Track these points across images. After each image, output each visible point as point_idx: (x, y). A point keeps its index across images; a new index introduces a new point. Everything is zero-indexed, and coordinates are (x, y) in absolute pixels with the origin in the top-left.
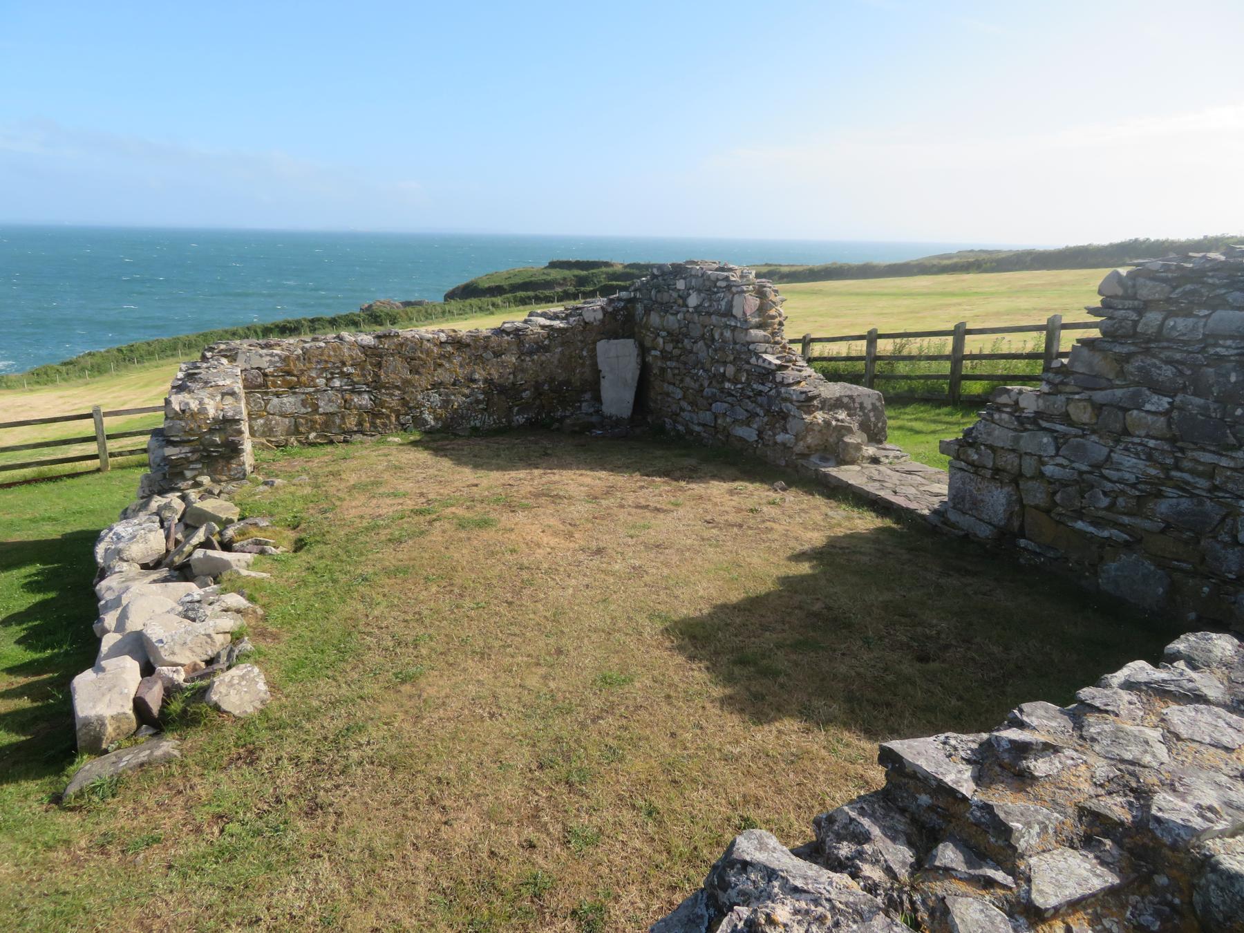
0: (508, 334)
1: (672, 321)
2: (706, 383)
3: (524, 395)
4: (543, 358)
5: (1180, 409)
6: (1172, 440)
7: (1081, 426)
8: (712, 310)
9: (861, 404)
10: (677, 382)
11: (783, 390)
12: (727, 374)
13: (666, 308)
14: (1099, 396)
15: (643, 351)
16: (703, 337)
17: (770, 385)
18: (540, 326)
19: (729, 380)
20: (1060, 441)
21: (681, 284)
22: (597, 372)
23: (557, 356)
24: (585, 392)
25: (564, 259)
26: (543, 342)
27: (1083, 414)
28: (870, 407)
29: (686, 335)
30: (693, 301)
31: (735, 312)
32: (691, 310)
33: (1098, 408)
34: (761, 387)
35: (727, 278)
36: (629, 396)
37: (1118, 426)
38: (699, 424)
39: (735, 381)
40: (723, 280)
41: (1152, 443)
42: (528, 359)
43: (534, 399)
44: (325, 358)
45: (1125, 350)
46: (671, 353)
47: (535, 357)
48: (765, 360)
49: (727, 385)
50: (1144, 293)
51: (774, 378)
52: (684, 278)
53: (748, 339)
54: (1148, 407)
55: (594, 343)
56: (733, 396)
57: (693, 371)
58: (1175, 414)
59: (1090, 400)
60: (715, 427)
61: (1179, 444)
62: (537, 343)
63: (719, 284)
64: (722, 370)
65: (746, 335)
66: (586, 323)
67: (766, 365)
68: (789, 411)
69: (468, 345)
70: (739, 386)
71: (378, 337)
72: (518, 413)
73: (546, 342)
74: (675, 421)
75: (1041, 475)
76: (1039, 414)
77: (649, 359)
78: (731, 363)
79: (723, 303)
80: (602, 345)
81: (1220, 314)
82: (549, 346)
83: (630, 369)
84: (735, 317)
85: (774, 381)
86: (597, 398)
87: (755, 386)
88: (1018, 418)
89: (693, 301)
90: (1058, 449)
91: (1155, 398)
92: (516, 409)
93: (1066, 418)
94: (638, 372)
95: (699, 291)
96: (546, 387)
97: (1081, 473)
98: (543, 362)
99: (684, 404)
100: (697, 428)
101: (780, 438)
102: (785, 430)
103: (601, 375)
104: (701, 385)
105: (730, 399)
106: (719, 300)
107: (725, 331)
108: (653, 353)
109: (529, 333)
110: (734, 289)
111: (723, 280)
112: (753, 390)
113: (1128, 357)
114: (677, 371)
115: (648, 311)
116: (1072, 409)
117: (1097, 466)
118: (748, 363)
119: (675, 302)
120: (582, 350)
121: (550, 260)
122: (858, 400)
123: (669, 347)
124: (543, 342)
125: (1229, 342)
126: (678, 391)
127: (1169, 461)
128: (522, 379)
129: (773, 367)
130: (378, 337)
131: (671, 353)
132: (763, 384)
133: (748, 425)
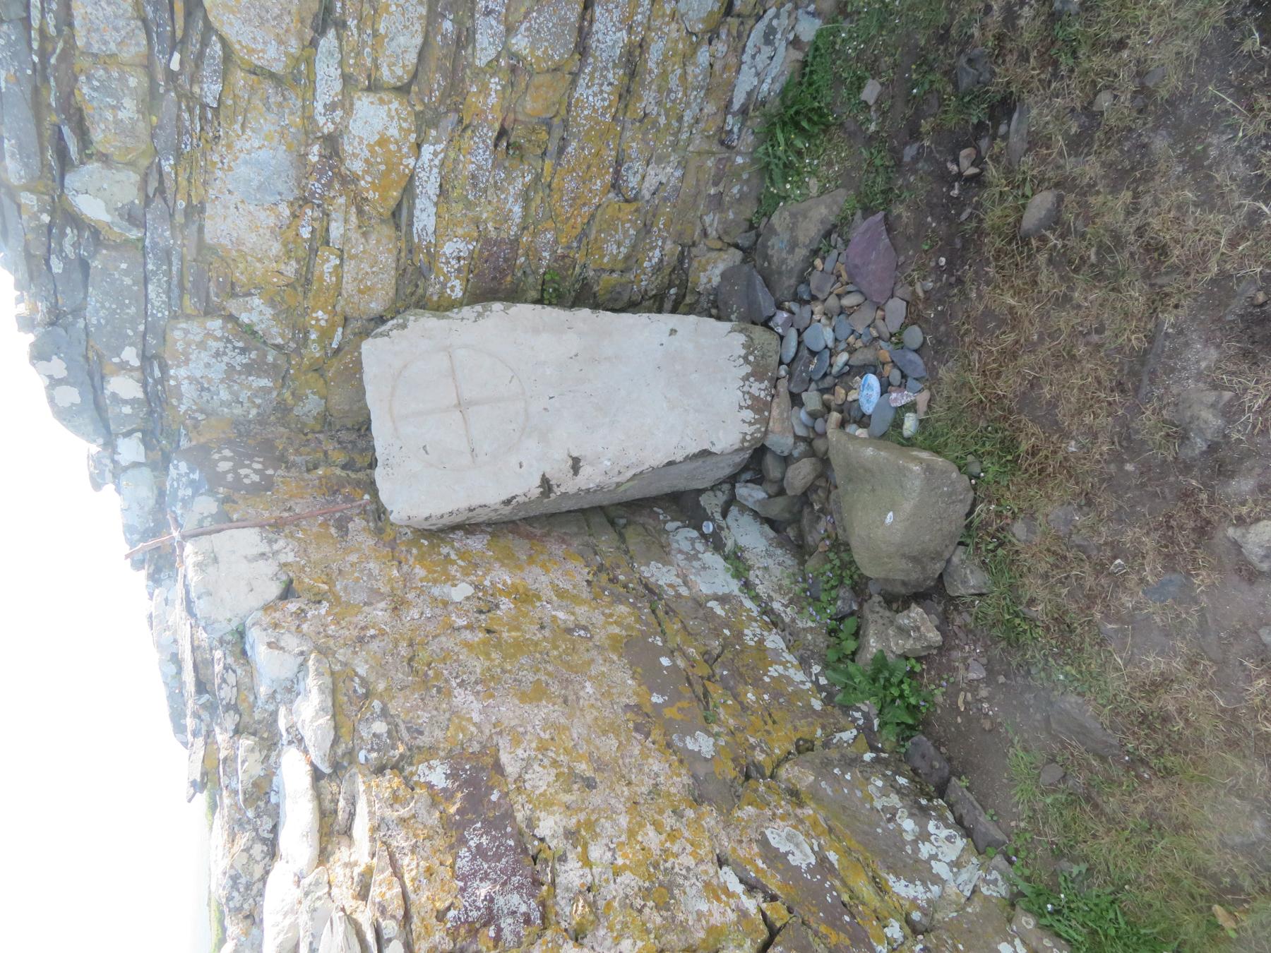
3: (802, 858)
4: (541, 779)
18: (323, 856)
23: (508, 710)
26: (437, 798)
42: (572, 874)
47: (549, 826)
62: (455, 829)
72: (920, 871)
73: (437, 776)
82: (455, 760)
92: (900, 887)
98: (569, 778)
109: (384, 890)
124: (437, 798)
128: (715, 891)
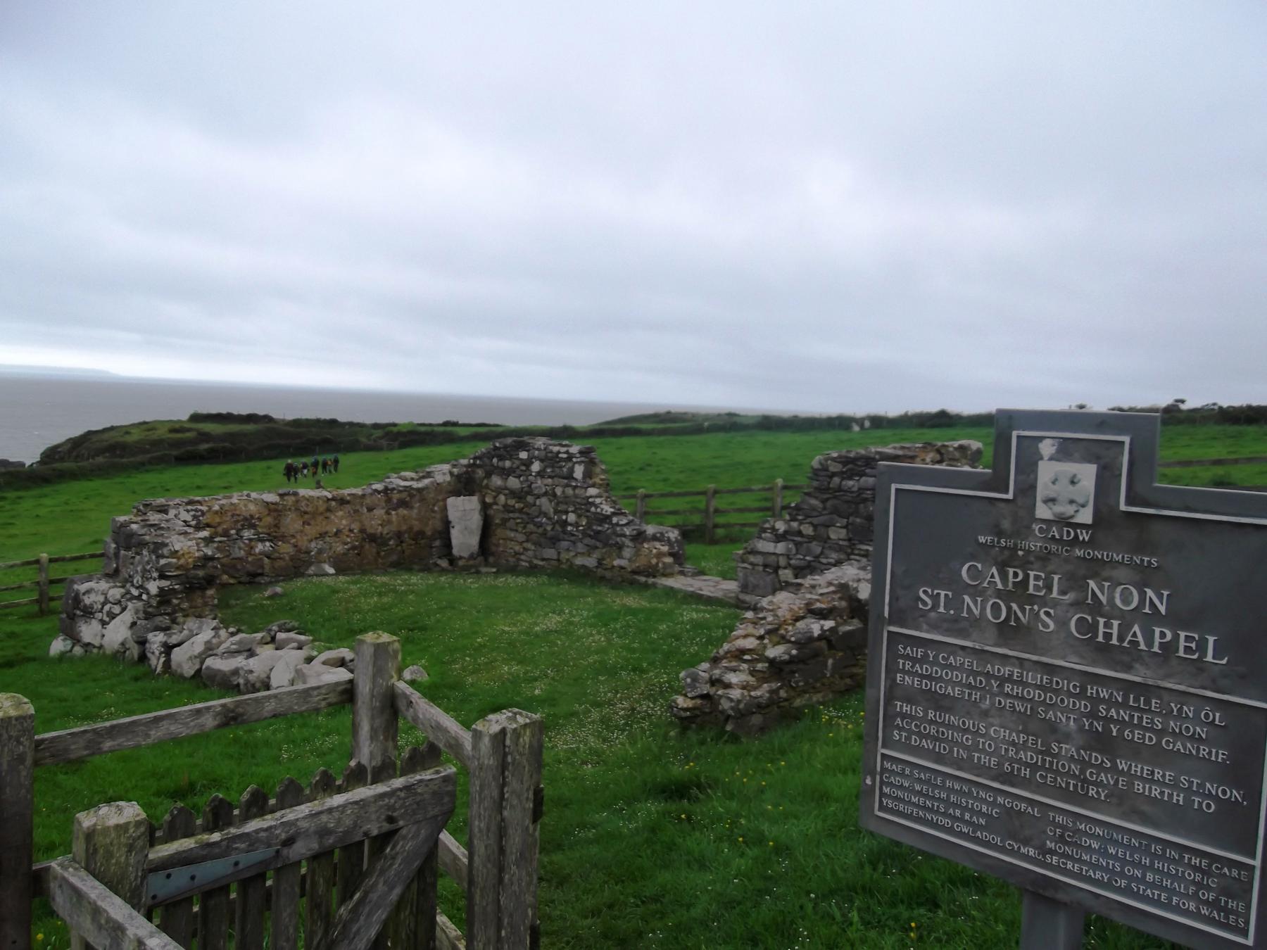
0: (379, 492)
1: (513, 482)
2: (549, 528)
5: (852, 524)
6: (850, 540)
7: (808, 537)
8: (553, 474)
9: (669, 538)
10: (520, 529)
11: (618, 529)
12: (569, 520)
13: (506, 473)
14: (815, 521)
15: (485, 507)
16: (546, 494)
17: (607, 526)
19: (571, 525)
20: (797, 544)
21: (523, 455)
22: (447, 524)
24: (435, 539)
25: (214, 411)
27: (808, 530)
28: (674, 540)
29: (530, 492)
30: (536, 467)
31: (575, 475)
32: (533, 474)
33: (815, 527)
34: (599, 528)
35: (567, 452)
36: (474, 541)
37: (825, 536)
38: (543, 560)
39: (577, 525)
40: (564, 453)
41: (841, 543)
43: (397, 546)
44: (238, 512)
45: (826, 496)
46: (514, 506)
48: (602, 510)
49: (569, 528)
50: (832, 469)
51: (611, 521)
52: (528, 451)
53: (588, 494)
54: (838, 525)
55: (445, 500)
56: (573, 535)
57: (536, 520)
58: (850, 527)
59: (811, 523)
60: (558, 560)
61: (853, 542)
63: (560, 455)
64: (564, 517)
65: (586, 492)
66: (438, 484)
67: (604, 512)
68: (623, 543)
69: (348, 502)
70: (581, 528)
71: (281, 496)
74: (519, 560)
75: (790, 565)
76: (786, 532)
77: (491, 512)
78: (572, 512)
79: (565, 470)
80: (451, 501)
81: (864, 479)
83: (476, 520)
84: (576, 480)
85: (610, 523)
86: (448, 545)
87: (595, 527)
88: (776, 535)
89: (536, 467)
90: (797, 550)
91: (840, 519)
93: (799, 533)
94: (481, 523)
95: (542, 461)
96: (406, 536)
97: (810, 562)
99: (529, 545)
100: (541, 563)
101: (616, 563)
102: (620, 557)
103: (452, 525)
104: (545, 530)
105: (573, 538)
106: (561, 467)
107: (566, 489)
108: (495, 507)
110: (574, 460)
111: (564, 453)
112: (593, 530)
113: (827, 499)
114: (519, 521)
115: (488, 475)
116: (802, 528)
117: (817, 557)
118: (588, 511)
119: (518, 468)
120: (434, 505)
121: (192, 412)
122: (666, 535)
123: (511, 502)
125: (868, 492)
126: (521, 535)
127: (849, 551)
129: (608, 513)
130: (281, 496)
131: (514, 506)
132: (600, 526)
133: (589, 556)
